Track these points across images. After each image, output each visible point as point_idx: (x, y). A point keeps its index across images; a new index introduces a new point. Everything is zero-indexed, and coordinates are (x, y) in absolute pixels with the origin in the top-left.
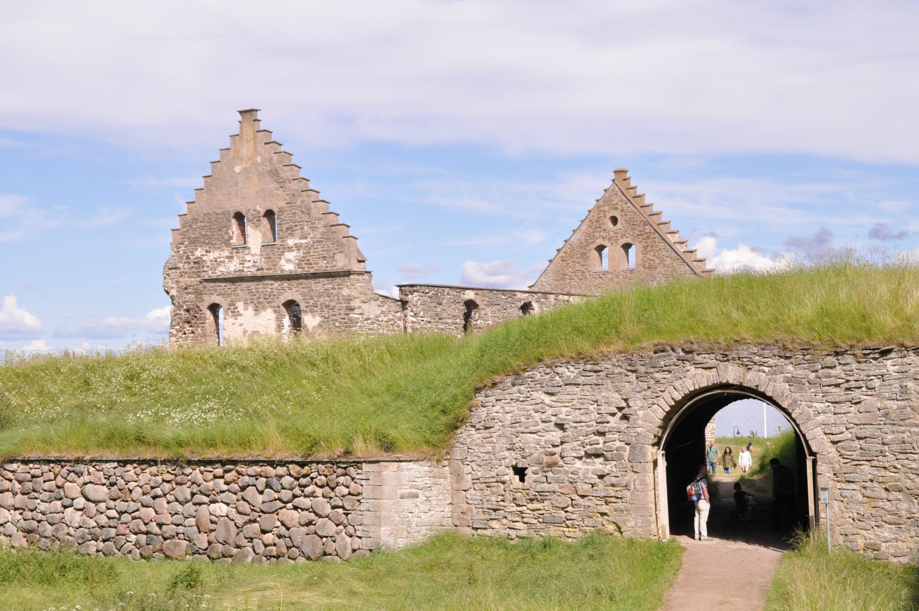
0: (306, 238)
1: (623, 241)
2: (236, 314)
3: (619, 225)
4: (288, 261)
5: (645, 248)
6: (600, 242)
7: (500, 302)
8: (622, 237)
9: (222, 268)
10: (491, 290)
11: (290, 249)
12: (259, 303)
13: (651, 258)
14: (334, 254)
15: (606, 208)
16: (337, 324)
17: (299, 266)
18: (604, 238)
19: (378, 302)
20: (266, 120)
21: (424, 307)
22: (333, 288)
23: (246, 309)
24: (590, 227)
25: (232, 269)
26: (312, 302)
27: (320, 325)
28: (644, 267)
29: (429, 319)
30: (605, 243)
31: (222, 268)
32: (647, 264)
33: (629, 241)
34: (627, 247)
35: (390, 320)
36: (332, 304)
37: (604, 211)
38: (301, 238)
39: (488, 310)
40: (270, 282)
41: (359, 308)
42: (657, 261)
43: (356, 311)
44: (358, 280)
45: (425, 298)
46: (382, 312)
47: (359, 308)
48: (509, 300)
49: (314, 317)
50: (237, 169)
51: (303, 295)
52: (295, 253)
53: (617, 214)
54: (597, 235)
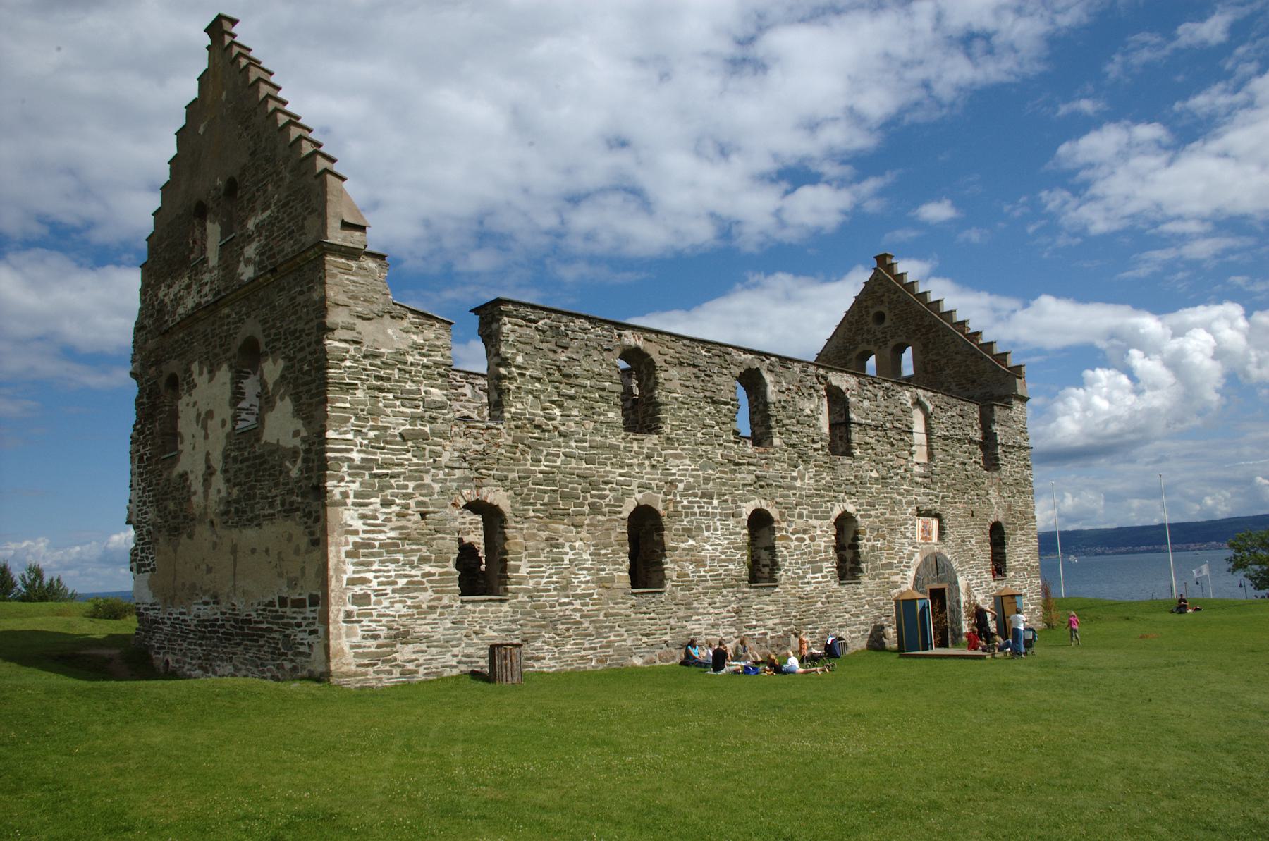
0: (269, 207)
1: (892, 343)
2: (192, 386)
3: (887, 323)
4: (248, 261)
5: (925, 346)
6: (862, 347)
7: (698, 361)
8: (892, 337)
9: (181, 310)
10: (680, 338)
11: (249, 239)
12: (216, 355)
13: (934, 358)
14: (305, 218)
15: (869, 303)
16: (306, 368)
17: (260, 266)
18: (868, 342)
19: (405, 324)
20: (243, 34)
21: (528, 349)
22: (301, 293)
23: (201, 374)
24: (850, 330)
25: (189, 307)
26: (273, 331)
27: (282, 376)
28: (926, 371)
29: (538, 374)
30: (871, 347)
31: (181, 310)
32: (929, 369)
33: (903, 339)
34: (900, 349)
35: (437, 365)
36: (300, 326)
37: (867, 307)
38: (264, 211)
39: (674, 372)
40: (226, 311)
41: (350, 328)
42: (944, 361)
43: (339, 333)
44: (347, 270)
45: (528, 331)
46: (416, 346)
47: (350, 328)
48: (716, 360)
49: (275, 362)
50: (201, 131)
51: (264, 321)
52: (254, 245)
53: (884, 309)
54: (858, 338)
